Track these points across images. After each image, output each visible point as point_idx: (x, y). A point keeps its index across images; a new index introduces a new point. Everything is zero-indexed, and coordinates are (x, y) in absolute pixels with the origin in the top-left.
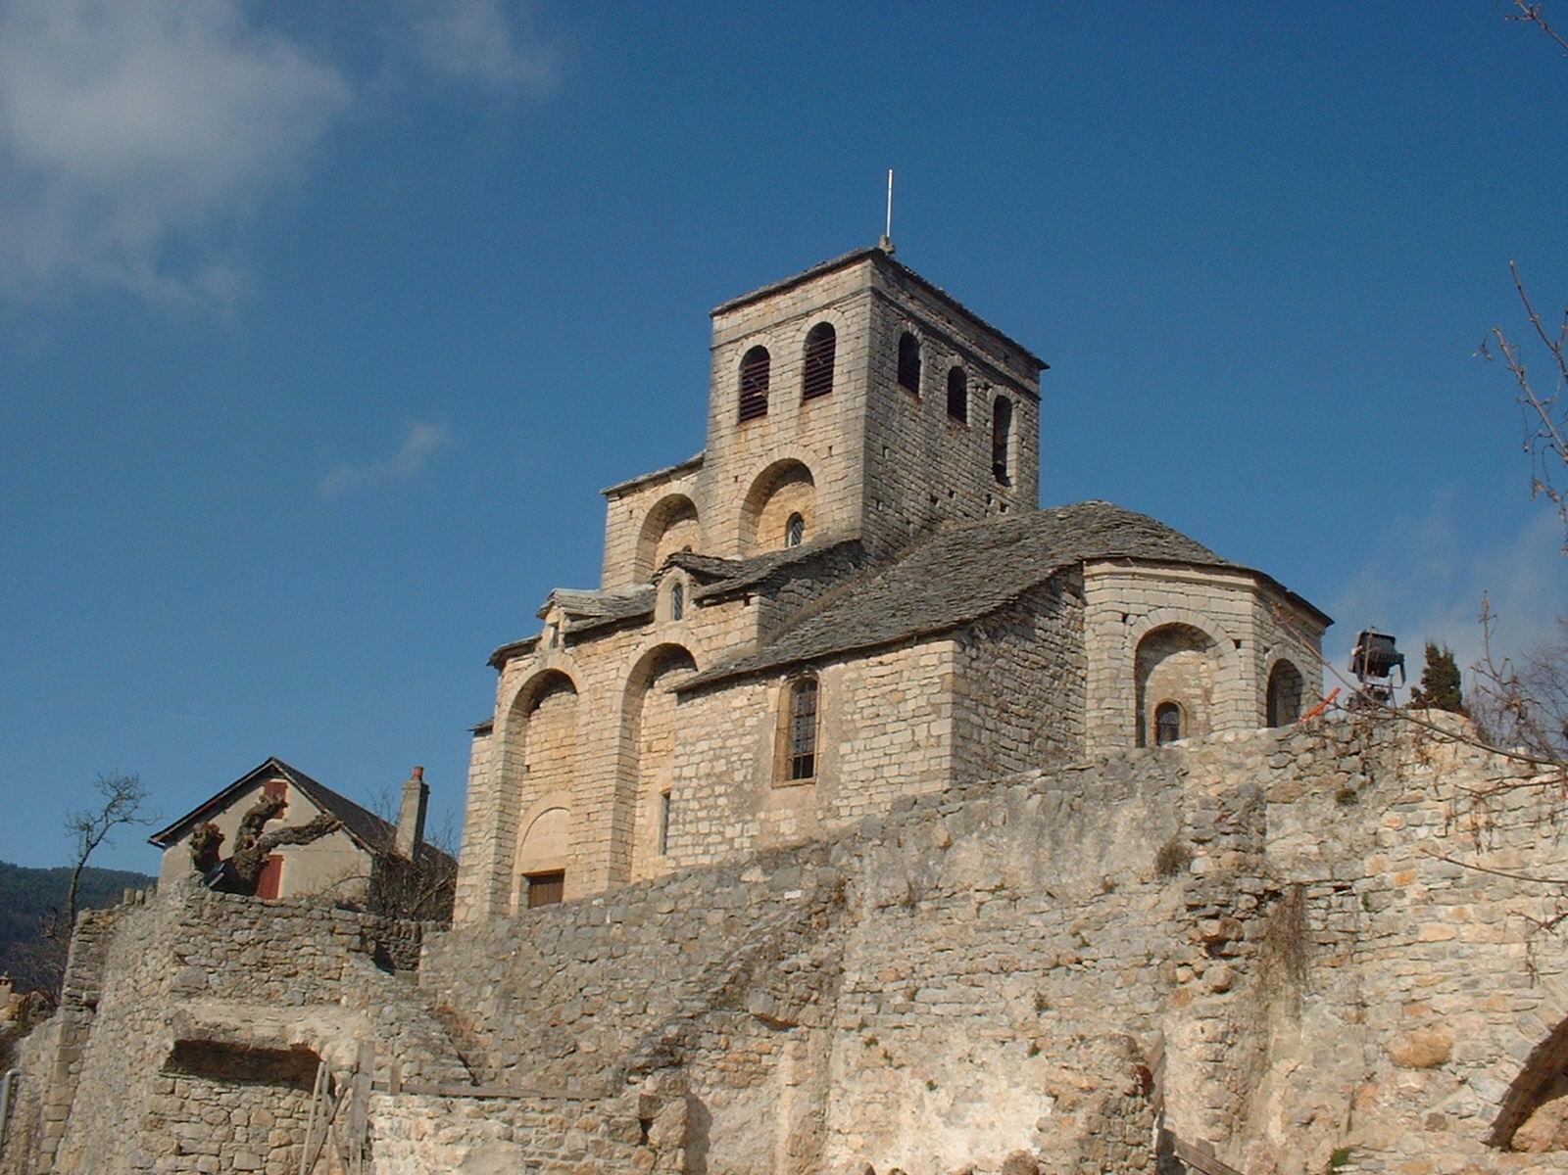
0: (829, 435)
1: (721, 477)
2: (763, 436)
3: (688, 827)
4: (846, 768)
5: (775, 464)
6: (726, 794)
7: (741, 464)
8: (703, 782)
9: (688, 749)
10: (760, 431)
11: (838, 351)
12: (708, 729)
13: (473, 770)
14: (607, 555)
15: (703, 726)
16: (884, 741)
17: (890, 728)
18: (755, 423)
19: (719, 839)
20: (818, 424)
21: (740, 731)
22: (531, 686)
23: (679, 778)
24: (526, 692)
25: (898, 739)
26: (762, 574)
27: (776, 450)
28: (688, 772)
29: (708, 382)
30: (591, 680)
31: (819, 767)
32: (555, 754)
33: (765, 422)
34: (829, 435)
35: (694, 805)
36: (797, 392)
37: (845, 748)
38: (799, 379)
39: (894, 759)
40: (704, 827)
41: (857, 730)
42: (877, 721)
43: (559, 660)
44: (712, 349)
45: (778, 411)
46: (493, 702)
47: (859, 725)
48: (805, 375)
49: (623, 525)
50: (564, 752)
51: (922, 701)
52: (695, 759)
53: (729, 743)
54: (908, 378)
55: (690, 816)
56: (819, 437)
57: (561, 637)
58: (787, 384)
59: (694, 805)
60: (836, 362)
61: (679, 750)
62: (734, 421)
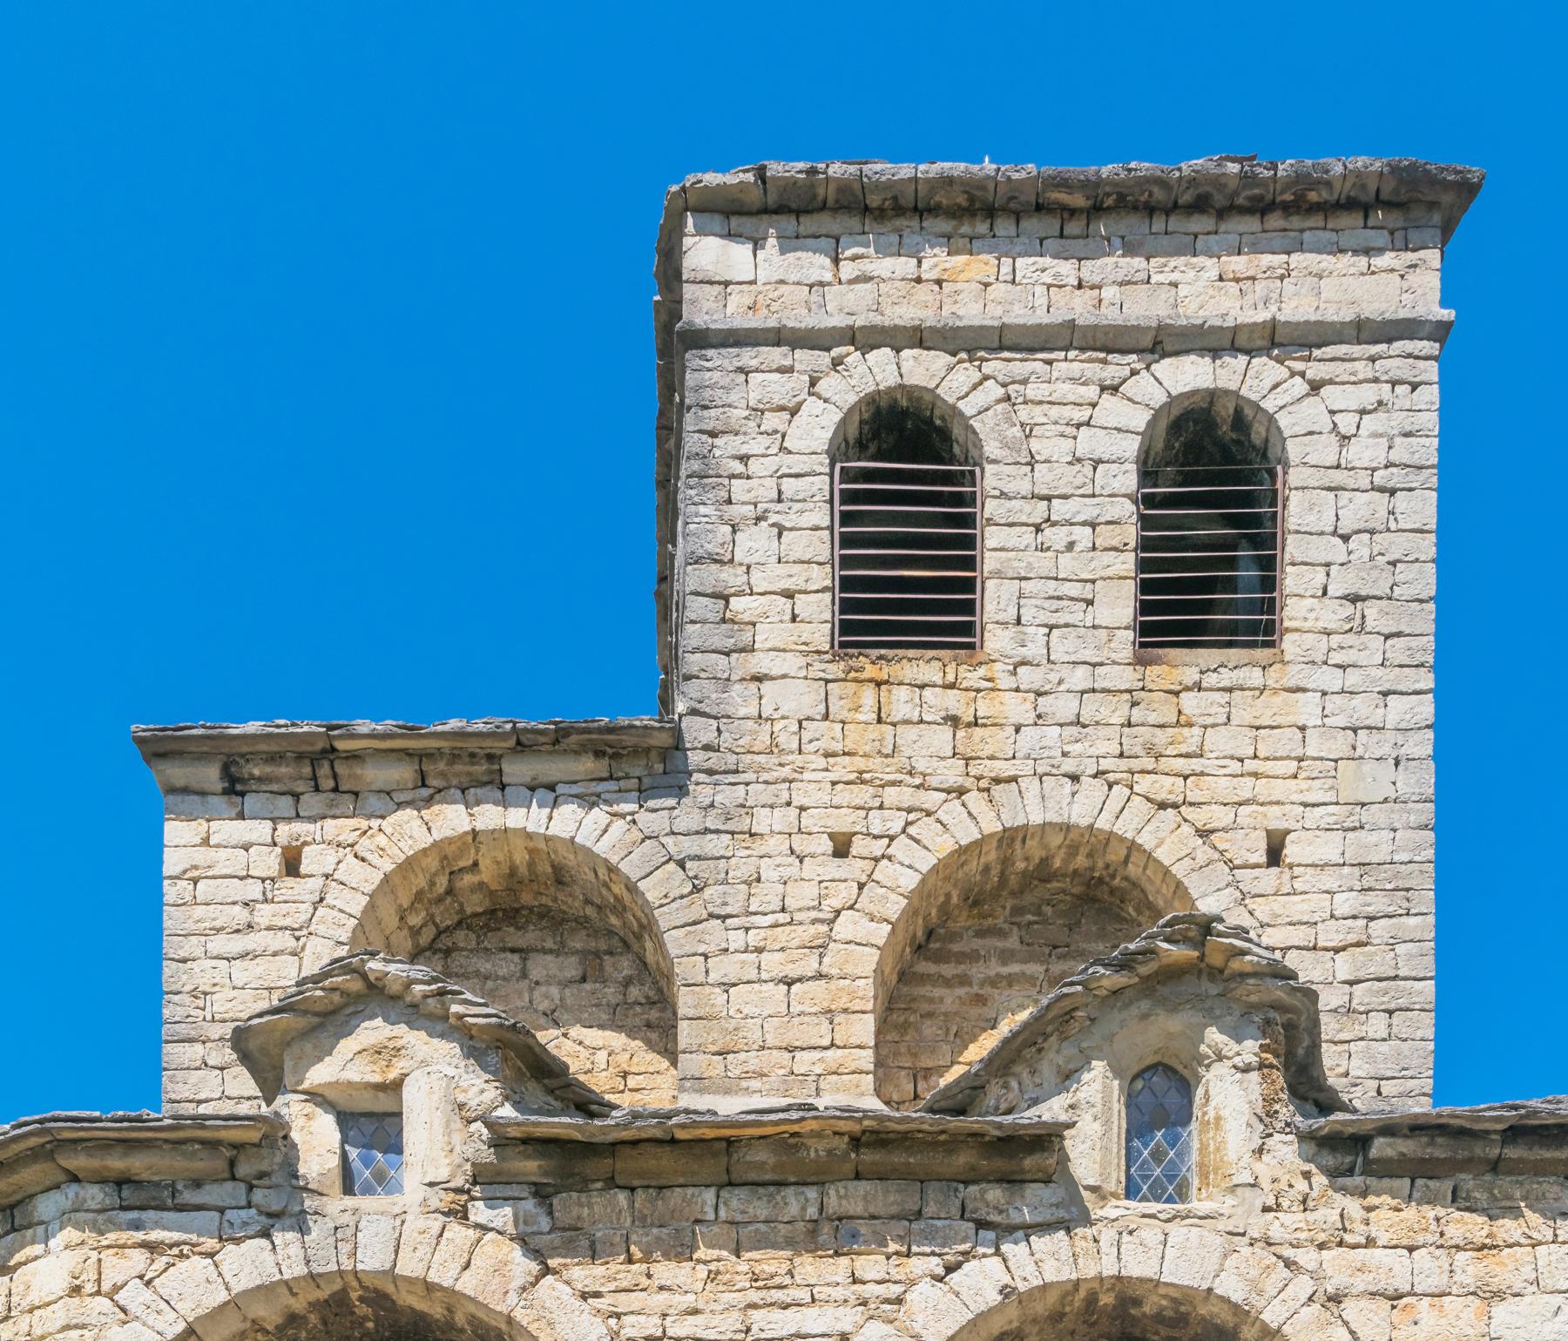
0: (1263, 789)
2: (953, 721)
5: (1010, 837)
7: (863, 795)
10: (954, 702)
18: (923, 667)
20: (1219, 741)
27: (1031, 787)
33: (972, 678)
34: (1263, 789)
38: (1126, 563)
45: (1035, 650)
49: (254, 890)
56: (1222, 787)
58: (1067, 564)
62: (820, 634)
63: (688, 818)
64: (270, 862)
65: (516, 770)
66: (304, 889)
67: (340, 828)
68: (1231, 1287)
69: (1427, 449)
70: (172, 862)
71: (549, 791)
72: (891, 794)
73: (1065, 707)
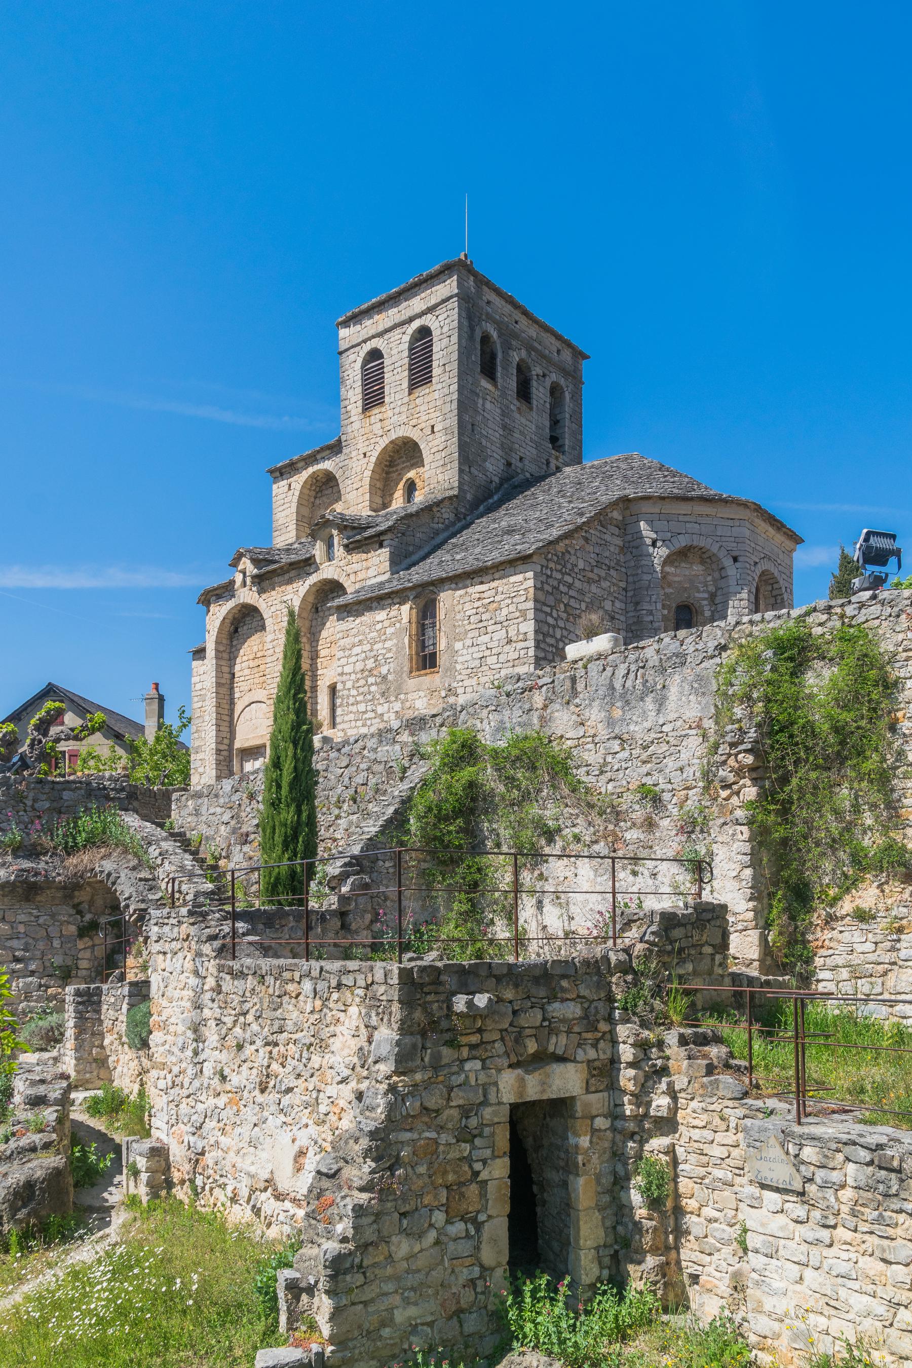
1: (354, 454)
3: (351, 708)
4: (460, 659)
6: (376, 684)
7: (367, 443)
8: (359, 676)
9: (347, 653)
10: (379, 416)
11: (435, 349)
12: (361, 638)
13: (194, 680)
14: (275, 517)
15: (355, 636)
16: (485, 638)
17: (490, 629)
18: (376, 411)
19: (372, 715)
21: (383, 638)
22: (230, 617)
23: (342, 674)
24: (227, 621)
25: (496, 636)
26: (390, 523)
28: (347, 669)
29: (337, 380)
30: (273, 609)
31: (443, 660)
32: (252, 664)
33: (383, 409)
35: (354, 692)
36: (405, 384)
37: (458, 645)
38: (406, 373)
39: (494, 651)
40: (362, 707)
41: (466, 632)
42: (481, 625)
43: (246, 595)
44: (341, 353)
46: (203, 630)
47: (468, 627)
48: (410, 370)
50: (257, 662)
51: (512, 608)
52: (353, 659)
53: (376, 647)
54: (489, 370)
55: (351, 700)
57: (248, 580)
59: (354, 692)
60: (434, 358)
61: (341, 654)
62: (360, 410)
63: (342, 457)
64: (286, 488)
65: (318, 457)
66: (291, 493)
67: (296, 478)
68: (336, 577)
69: (456, 324)
70: (274, 494)
71: (323, 459)
72: (372, 441)
73: (397, 411)
